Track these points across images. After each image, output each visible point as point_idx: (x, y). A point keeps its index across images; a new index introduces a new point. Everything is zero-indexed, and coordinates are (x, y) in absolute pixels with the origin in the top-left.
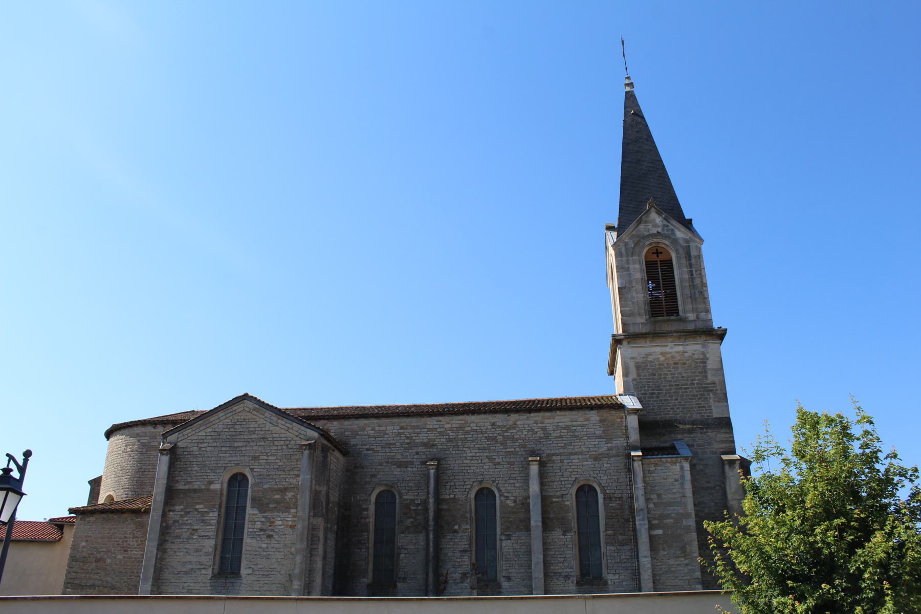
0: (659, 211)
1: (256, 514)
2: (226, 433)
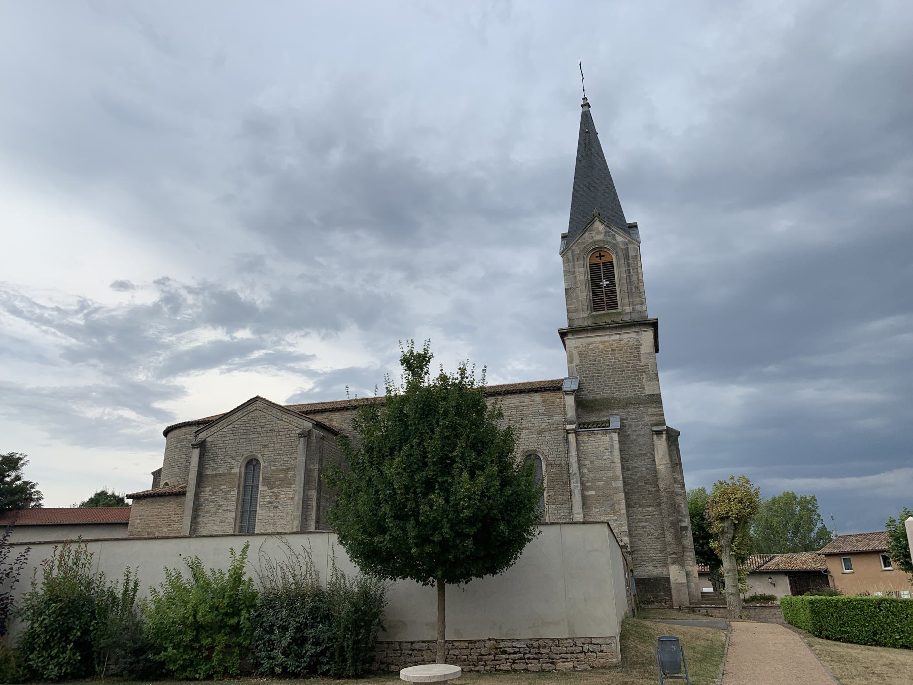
1: (266, 491)
2: (243, 428)
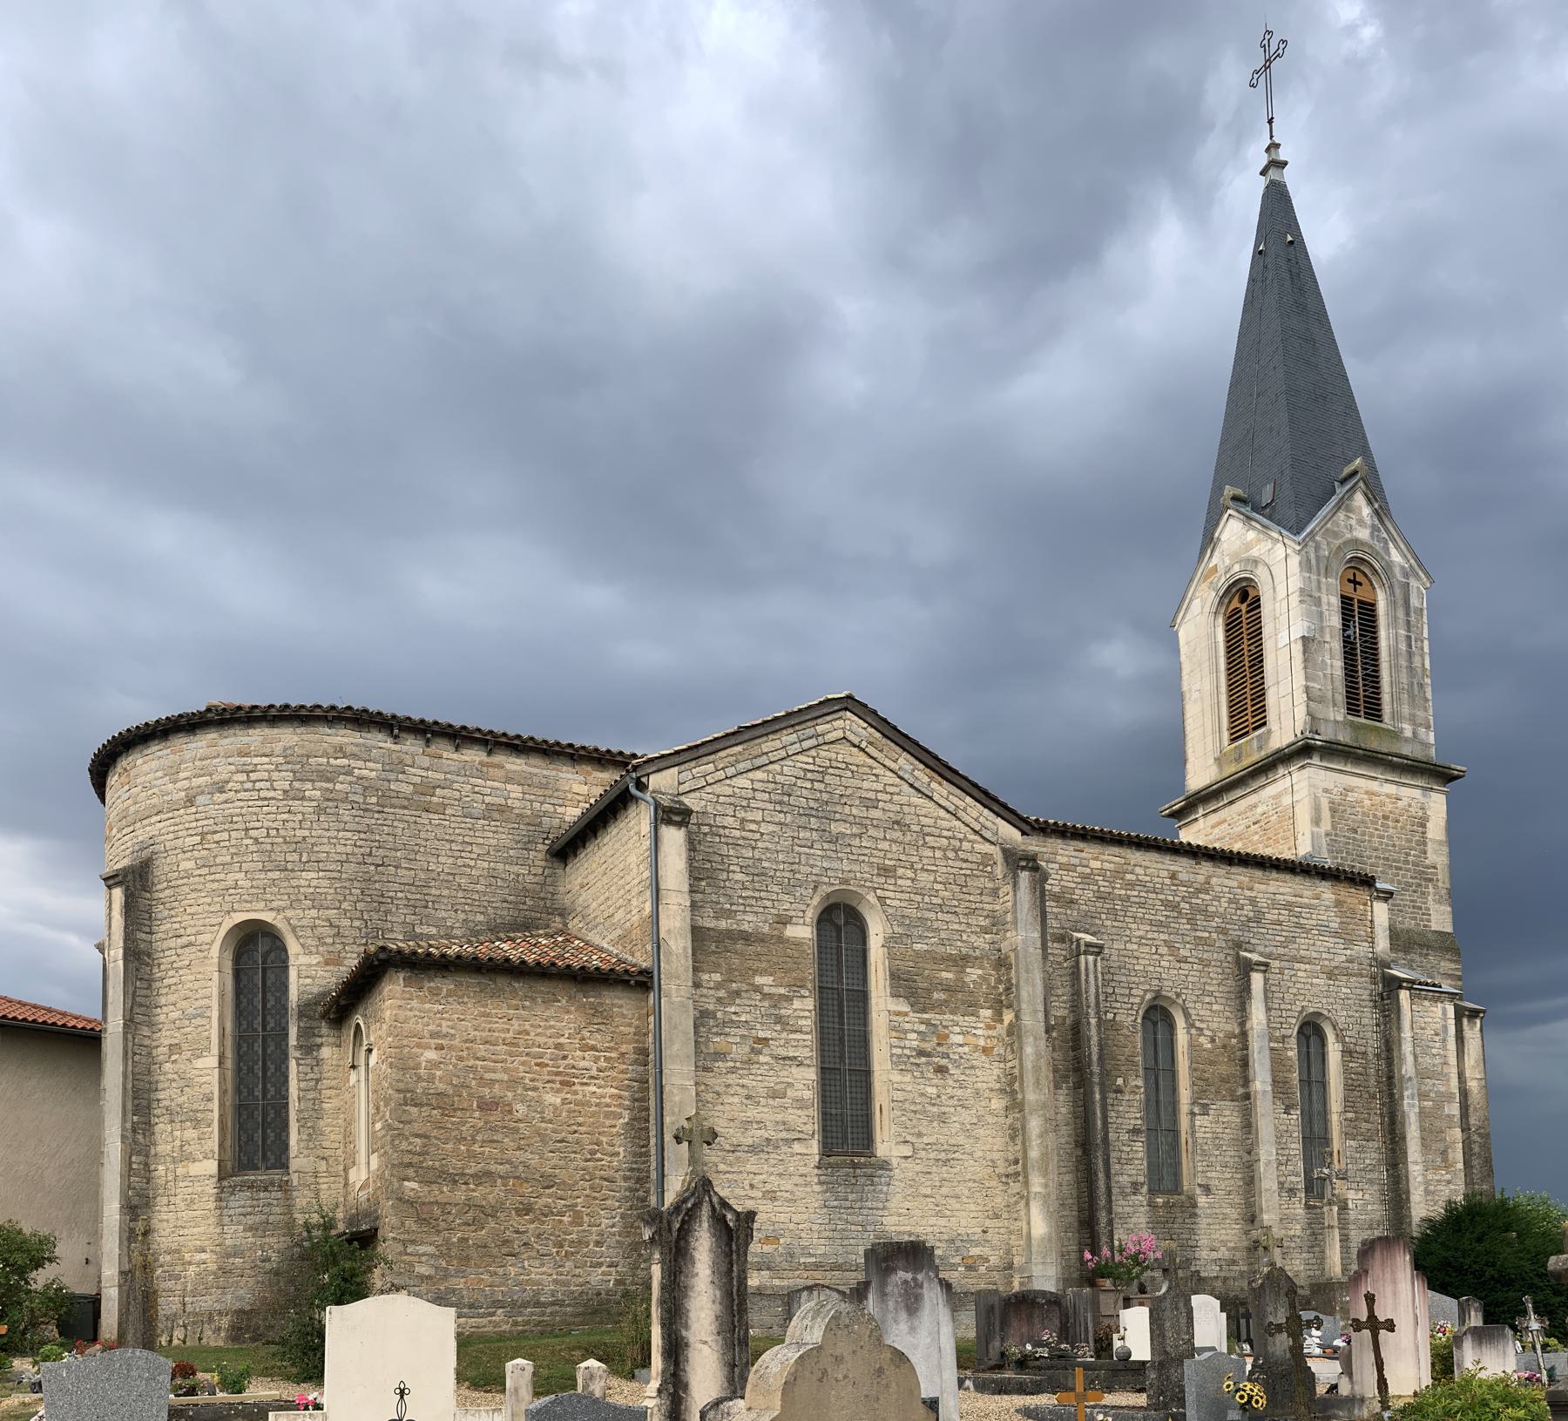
1: (906, 1014)
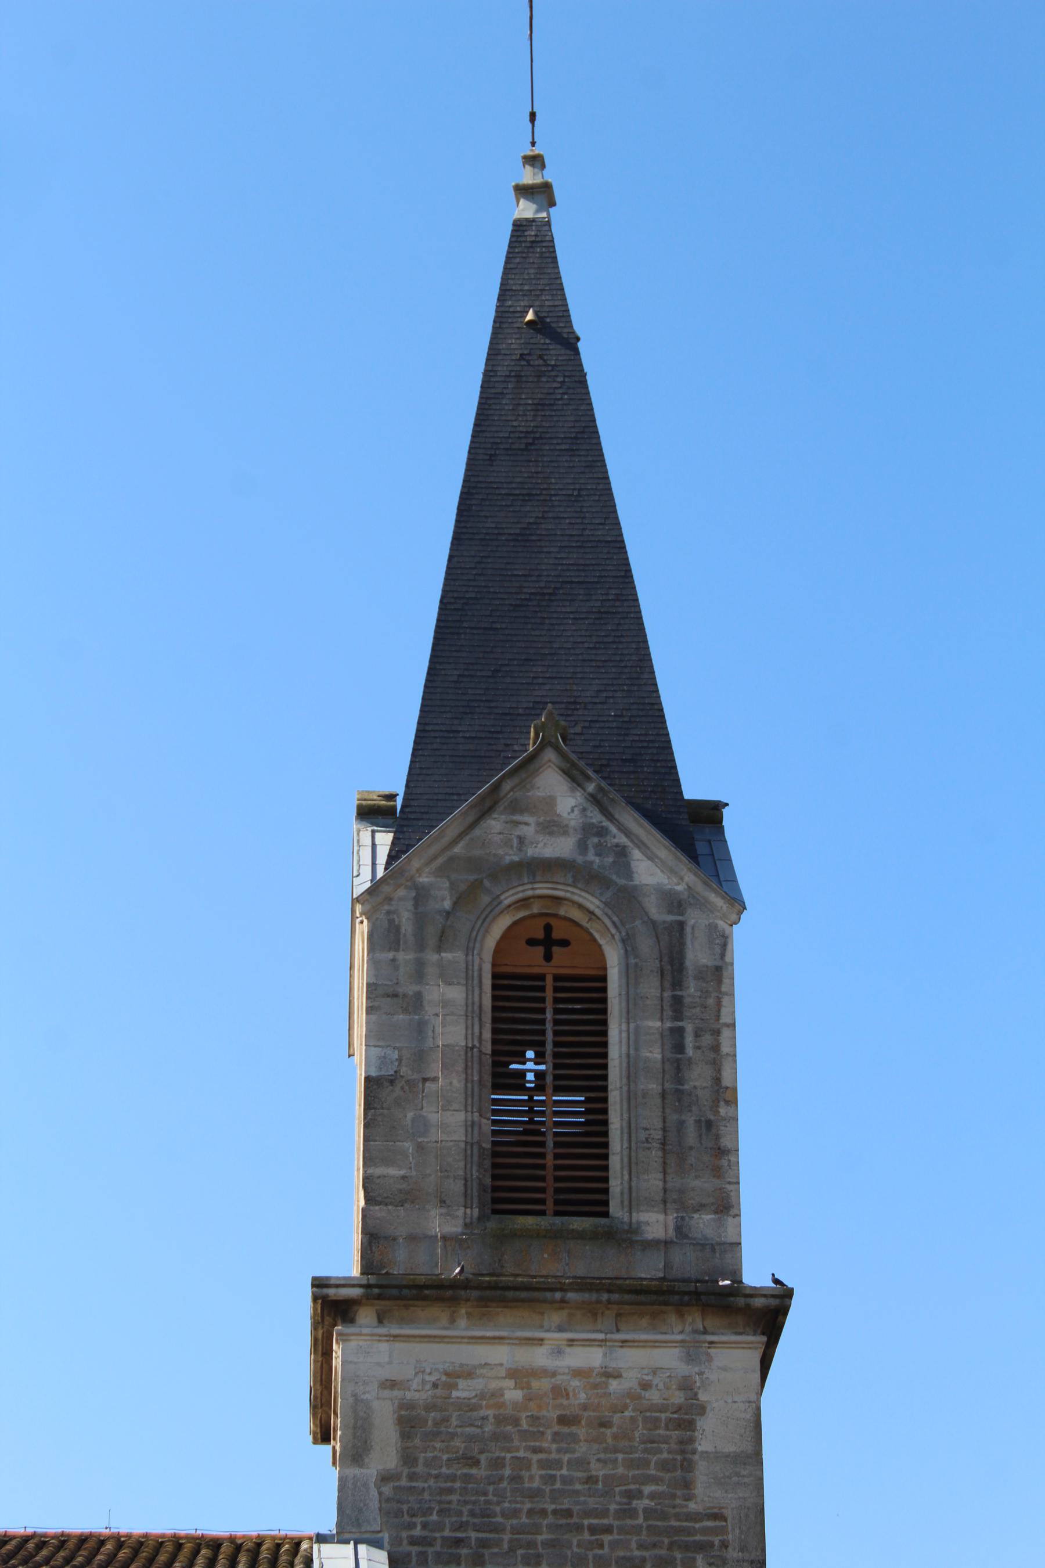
0: (573, 765)
